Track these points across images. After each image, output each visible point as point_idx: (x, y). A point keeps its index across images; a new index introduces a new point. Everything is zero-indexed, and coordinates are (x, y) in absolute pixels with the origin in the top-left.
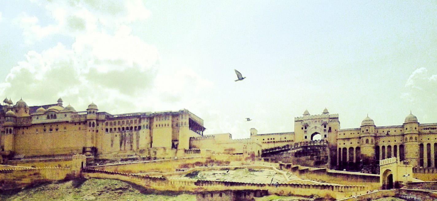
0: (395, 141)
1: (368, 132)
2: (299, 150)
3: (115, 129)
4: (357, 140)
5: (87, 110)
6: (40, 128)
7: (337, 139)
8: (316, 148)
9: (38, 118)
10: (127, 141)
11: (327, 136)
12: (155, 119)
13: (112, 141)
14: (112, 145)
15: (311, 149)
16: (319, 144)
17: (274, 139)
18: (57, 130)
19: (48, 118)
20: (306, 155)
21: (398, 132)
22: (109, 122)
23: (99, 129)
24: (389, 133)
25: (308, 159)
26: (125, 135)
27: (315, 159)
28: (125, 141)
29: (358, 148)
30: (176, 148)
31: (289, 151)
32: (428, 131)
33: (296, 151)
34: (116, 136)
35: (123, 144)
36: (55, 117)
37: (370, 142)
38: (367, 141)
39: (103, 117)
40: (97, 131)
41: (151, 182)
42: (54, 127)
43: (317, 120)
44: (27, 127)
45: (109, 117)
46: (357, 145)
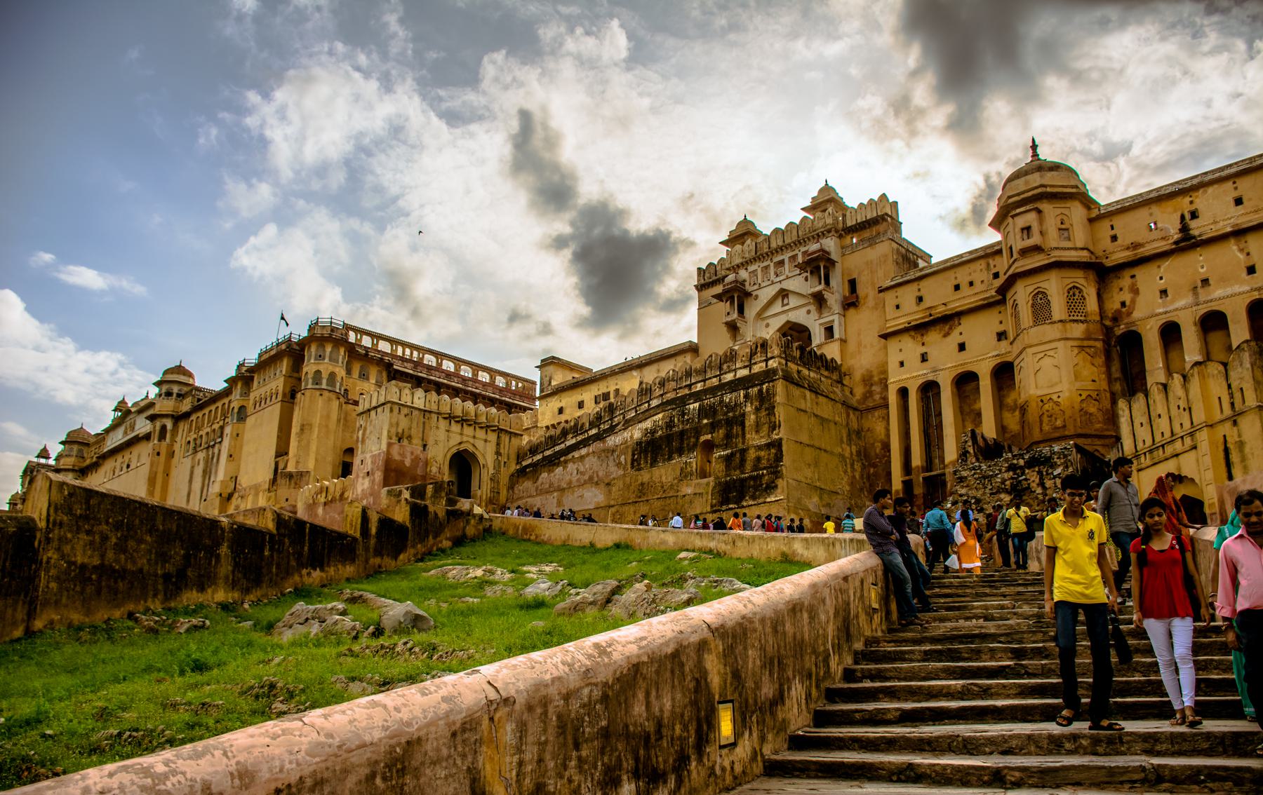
0: (1251, 270)
1: (1035, 240)
2: (648, 424)
5: (158, 384)
7: (885, 337)
8: (727, 398)
11: (837, 335)
15: (703, 412)
16: (745, 372)
18: (128, 466)
20: (680, 452)
23: (177, 447)
24: (1196, 228)
25: (684, 475)
27: (717, 467)
29: (1004, 374)
31: (612, 441)
33: (636, 433)
37: (1058, 308)
38: (1041, 310)
39: (186, 406)
43: (786, 256)
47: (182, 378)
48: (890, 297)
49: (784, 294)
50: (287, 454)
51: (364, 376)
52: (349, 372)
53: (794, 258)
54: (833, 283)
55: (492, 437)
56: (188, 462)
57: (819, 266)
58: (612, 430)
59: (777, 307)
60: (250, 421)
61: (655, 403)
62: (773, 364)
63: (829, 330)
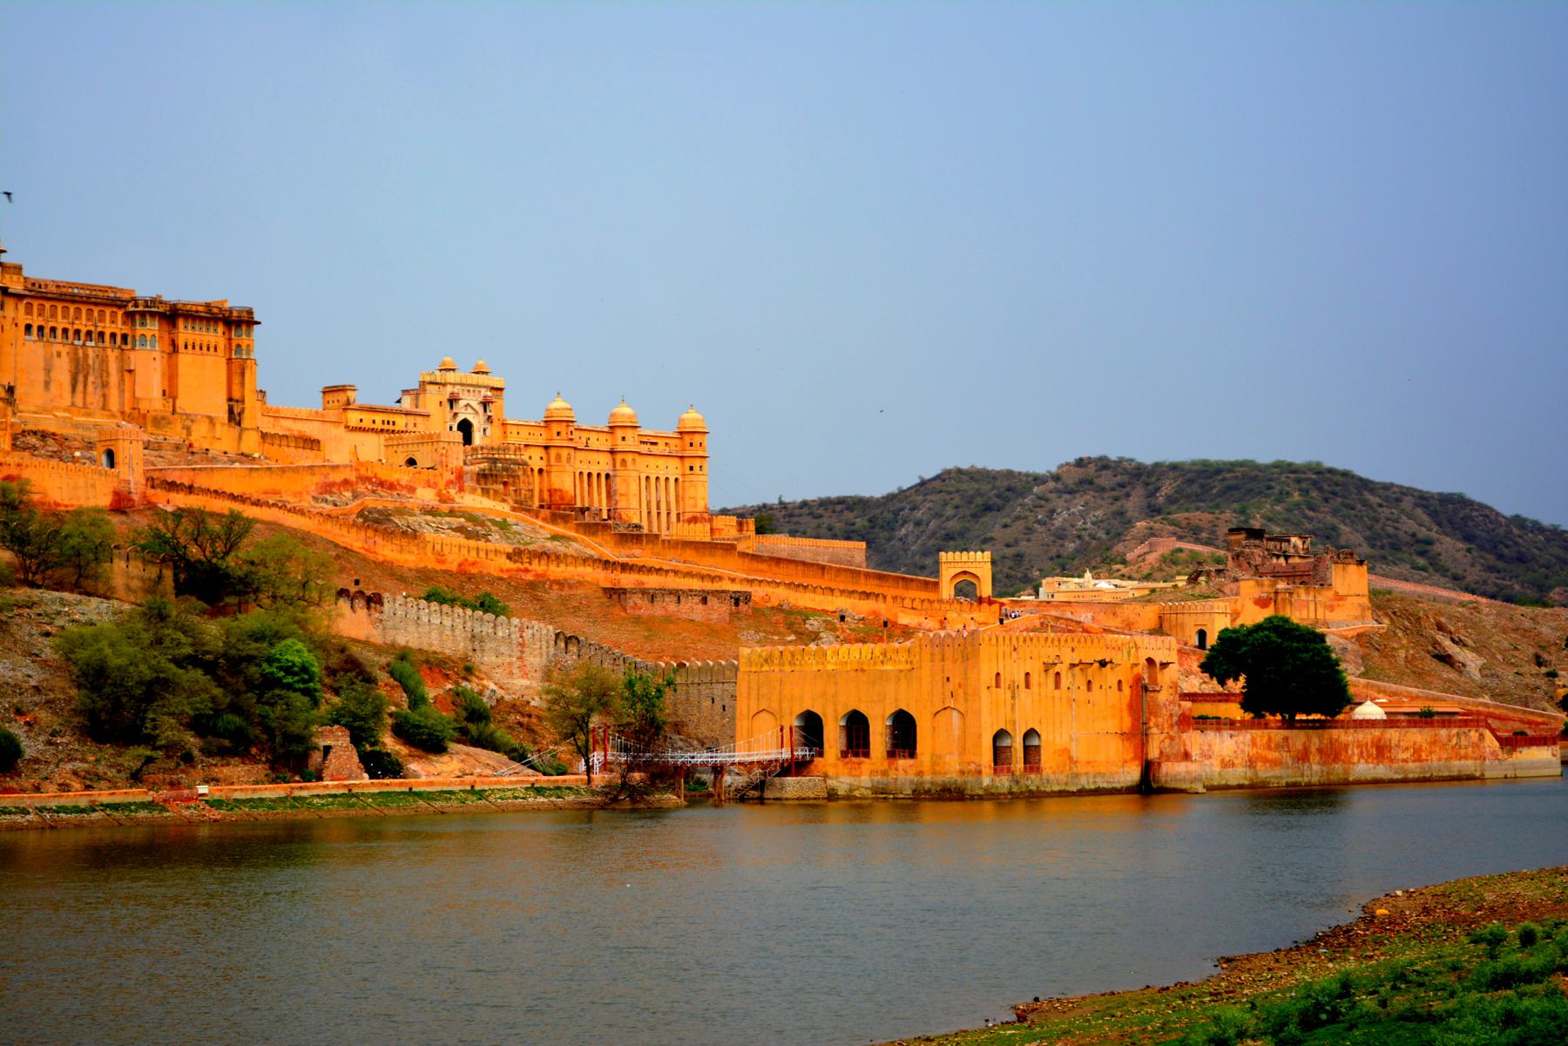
3: (53, 330)
4: (541, 452)
10: (91, 379)
12: (181, 323)
13: (48, 371)
14: (47, 384)
15: (504, 469)
21: (603, 443)
22: (36, 303)
26: (86, 356)
28: (86, 378)
30: (239, 424)
32: (644, 449)
34: (59, 355)
35: (80, 387)
41: (379, 540)
46: (542, 464)
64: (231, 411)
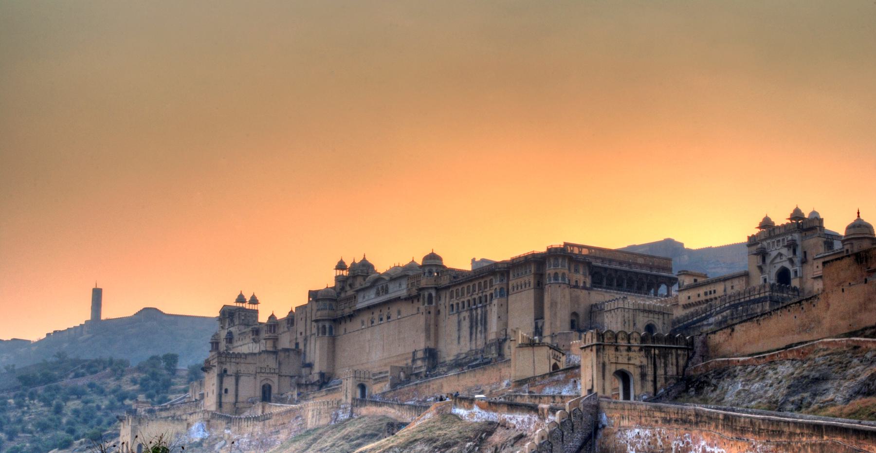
6: (366, 317)
9: (364, 297)
10: (479, 329)
14: (459, 338)
17: (715, 291)
18: (389, 318)
19: (378, 294)
23: (442, 308)
34: (464, 319)
36: (387, 292)
39: (445, 281)
40: (438, 312)
42: (385, 312)
43: (781, 238)
44: (351, 317)
45: (458, 278)
47: (437, 262)
48: (815, 262)
49: (780, 255)
50: (542, 318)
51: (576, 271)
52: (569, 269)
53: (783, 240)
54: (797, 253)
55: (661, 317)
56: (455, 318)
57: (792, 246)
58: (711, 315)
59: (778, 260)
60: (512, 298)
61: (727, 305)
62: (767, 294)
63: (796, 272)
64: (536, 327)
